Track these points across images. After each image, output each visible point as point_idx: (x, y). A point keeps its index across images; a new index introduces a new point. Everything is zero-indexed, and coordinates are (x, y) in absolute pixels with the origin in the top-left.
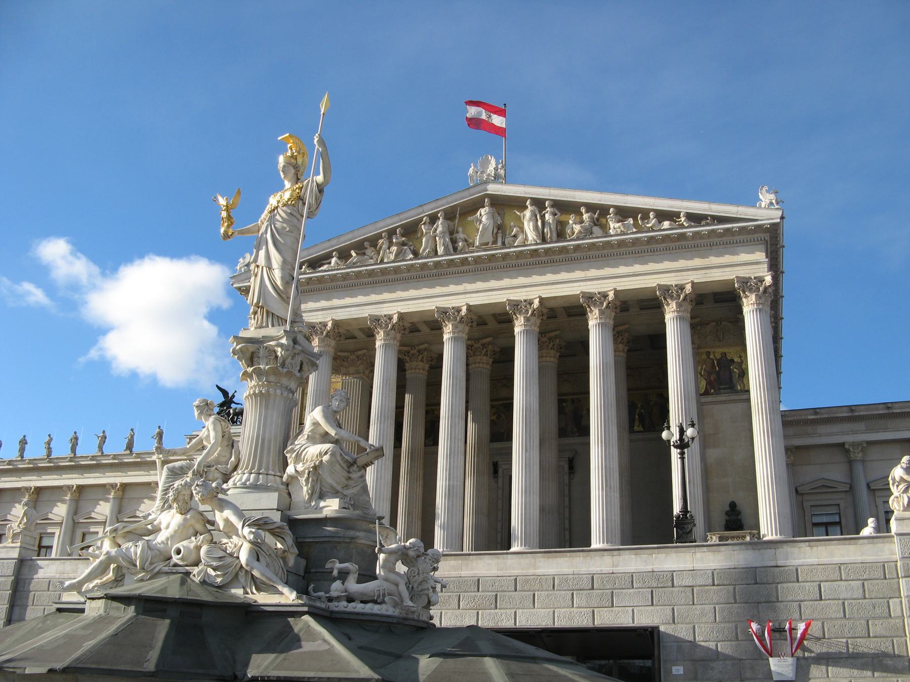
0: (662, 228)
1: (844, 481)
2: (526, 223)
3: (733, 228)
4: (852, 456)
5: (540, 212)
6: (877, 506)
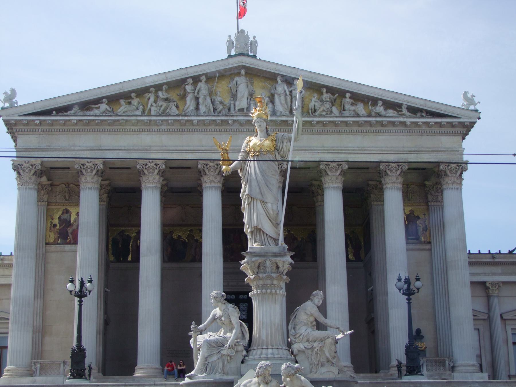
0: (387, 115)
1: (482, 311)
2: (276, 96)
4: (490, 292)
5: (288, 88)
6: (507, 332)
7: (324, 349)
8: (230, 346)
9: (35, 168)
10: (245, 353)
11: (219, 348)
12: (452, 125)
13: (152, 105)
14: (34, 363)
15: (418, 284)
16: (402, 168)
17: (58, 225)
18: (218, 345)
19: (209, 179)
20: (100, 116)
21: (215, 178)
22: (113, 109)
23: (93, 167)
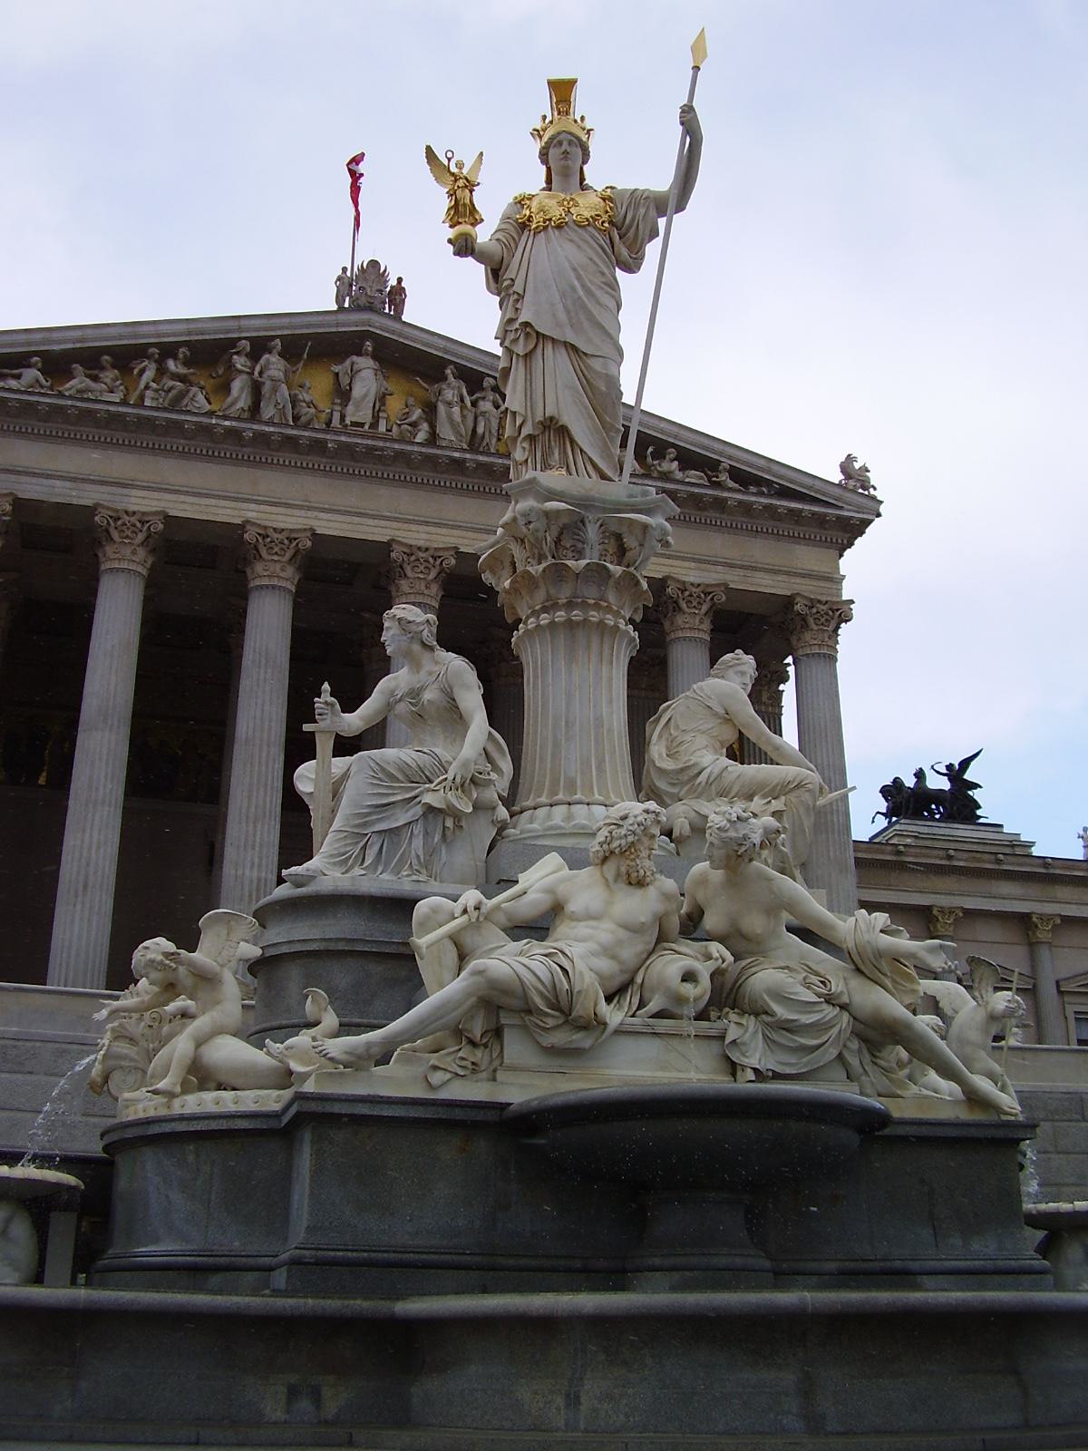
0: (687, 480)
2: (441, 408)
3: (801, 511)
5: (471, 393)
10: (502, 812)
12: (821, 521)
13: (147, 387)
16: (712, 599)
19: (267, 570)
22: (52, 385)
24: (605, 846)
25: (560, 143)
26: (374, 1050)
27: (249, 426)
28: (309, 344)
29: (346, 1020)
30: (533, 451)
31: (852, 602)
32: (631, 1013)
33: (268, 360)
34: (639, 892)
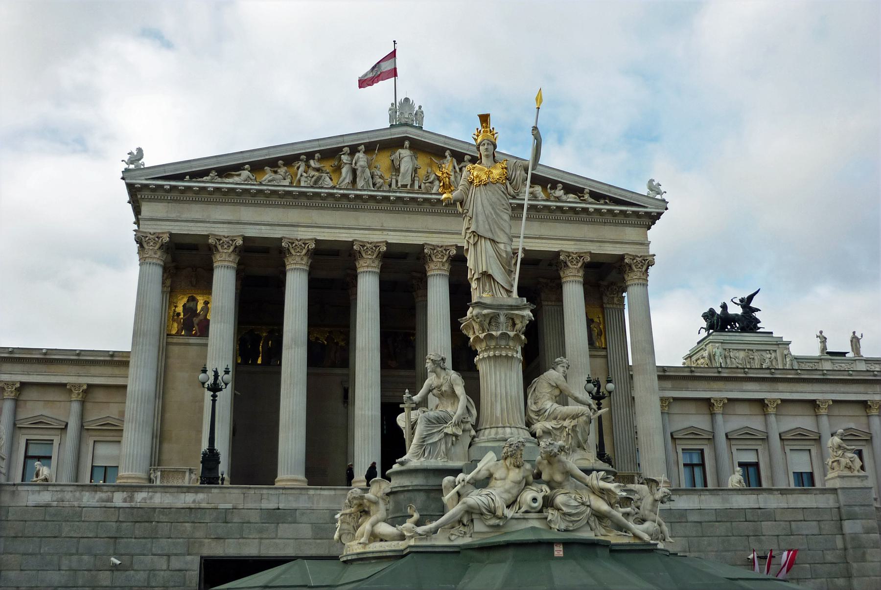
3: (626, 211)
5: (457, 164)
6: (677, 452)
7: (578, 429)
8: (456, 423)
9: (162, 240)
10: (473, 433)
11: (441, 425)
13: (301, 176)
14: (154, 471)
15: (610, 386)
16: (583, 260)
17: (182, 314)
18: (439, 421)
19: (366, 263)
20: (242, 184)
21: (373, 262)
22: (256, 178)
23: (230, 242)
24: (506, 454)
25: (484, 144)
26: (433, 530)
27: (352, 192)
28: (378, 146)
29: (421, 514)
30: (478, 285)
31: (654, 255)
32: (516, 512)
33: (359, 158)
34: (517, 470)
